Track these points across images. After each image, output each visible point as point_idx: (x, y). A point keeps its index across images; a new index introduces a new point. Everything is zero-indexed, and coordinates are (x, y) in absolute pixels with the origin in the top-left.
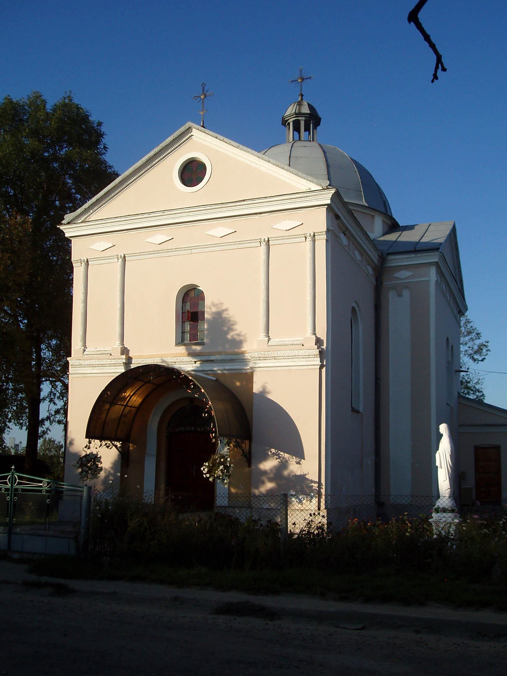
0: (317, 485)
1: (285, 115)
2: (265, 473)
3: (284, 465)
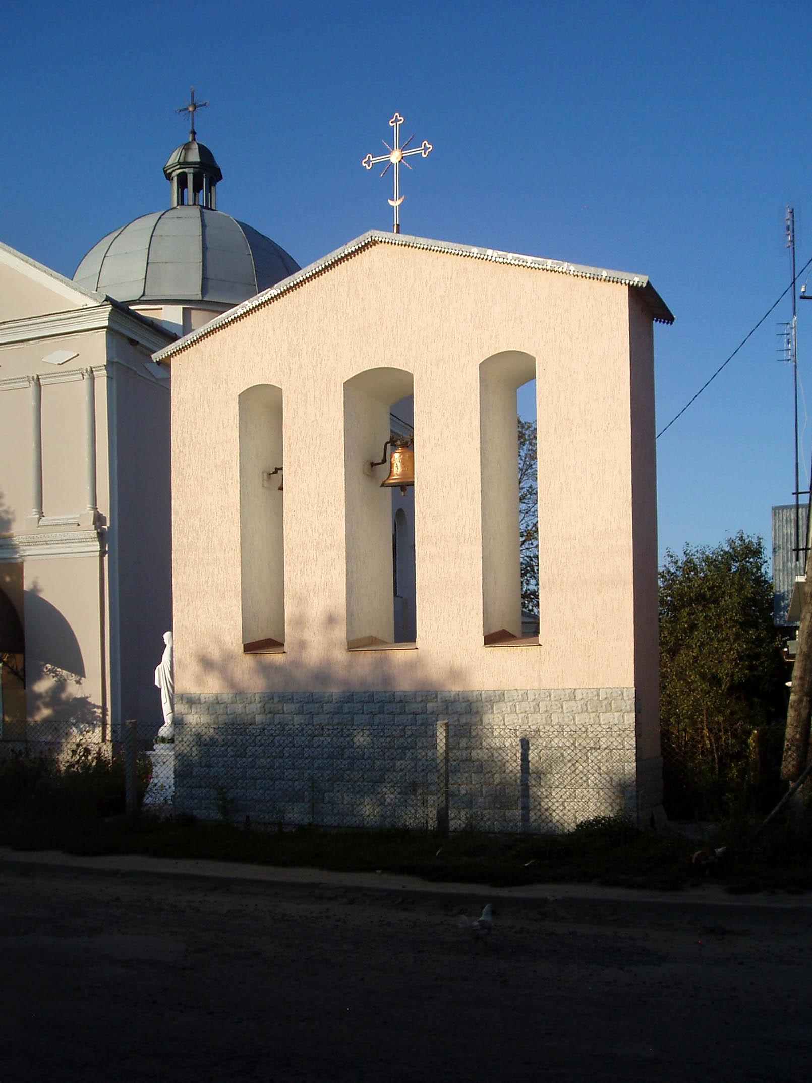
0: (100, 711)
1: (168, 165)
2: (39, 696)
3: (61, 686)
